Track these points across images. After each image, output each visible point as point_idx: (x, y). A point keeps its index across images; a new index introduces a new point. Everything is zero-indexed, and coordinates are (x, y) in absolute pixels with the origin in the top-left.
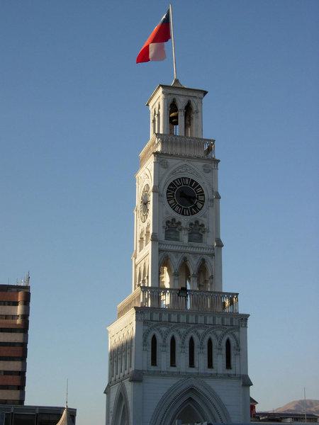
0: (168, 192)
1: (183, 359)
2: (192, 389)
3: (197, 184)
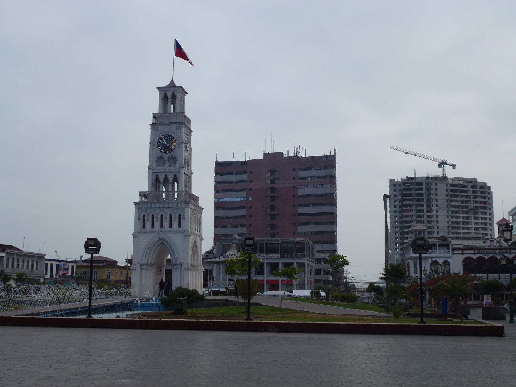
1: (157, 224)
2: (161, 239)
3: (172, 136)
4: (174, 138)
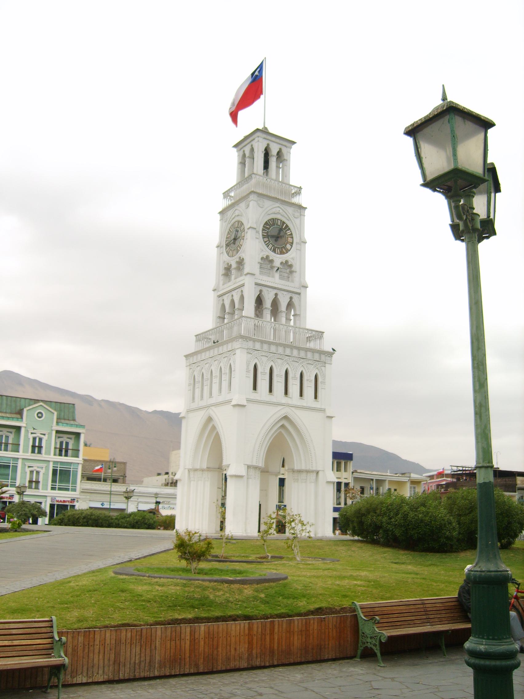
0: (263, 230)
2: (286, 418)
3: (287, 226)
4: (289, 229)
